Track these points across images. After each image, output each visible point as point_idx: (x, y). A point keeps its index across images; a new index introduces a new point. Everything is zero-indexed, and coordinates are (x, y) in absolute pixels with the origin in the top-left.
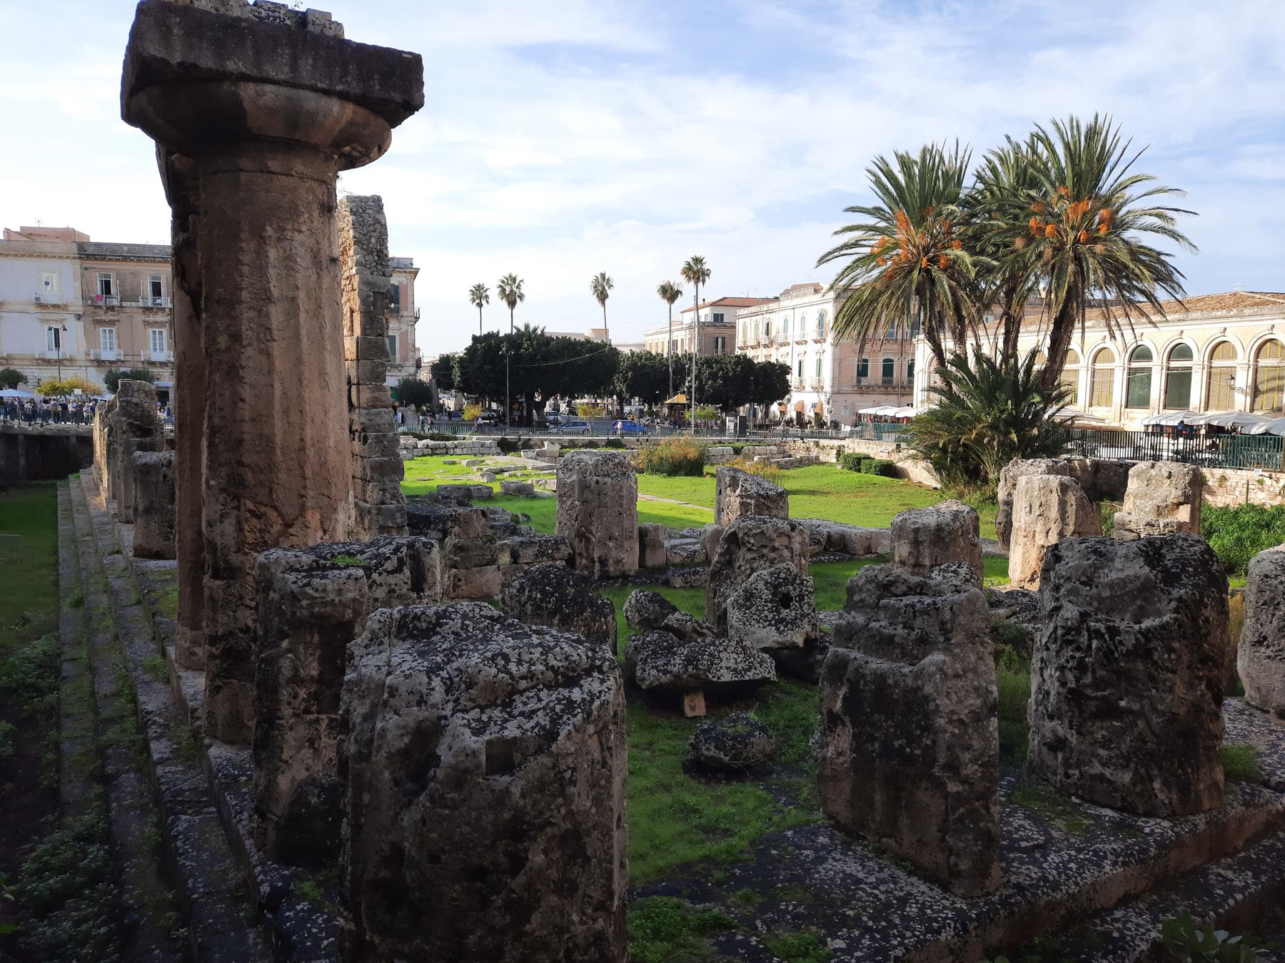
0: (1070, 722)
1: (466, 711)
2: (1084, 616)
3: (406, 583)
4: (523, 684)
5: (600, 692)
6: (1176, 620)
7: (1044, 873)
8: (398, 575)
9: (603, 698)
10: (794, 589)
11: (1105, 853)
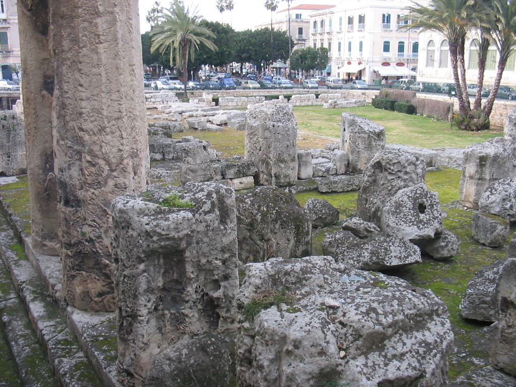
4: (390, 331)
10: (427, 201)
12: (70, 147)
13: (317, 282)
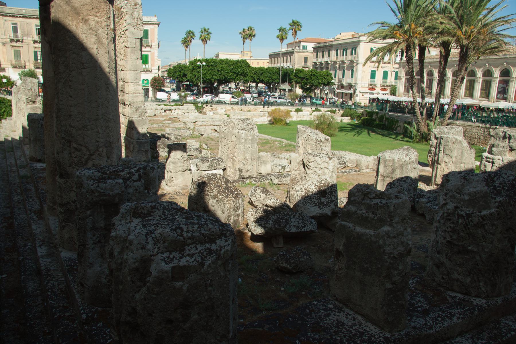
0: (446, 255)
1: (162, 253)
2: (456, 208)
3: (142, 186)
5: (225, 246)
6: (497, 211)
7: (426, 322)
8: (138, 182)
9: (226, 249)
11: (455, 313)
12: (63, 138)
13: (159, 214)
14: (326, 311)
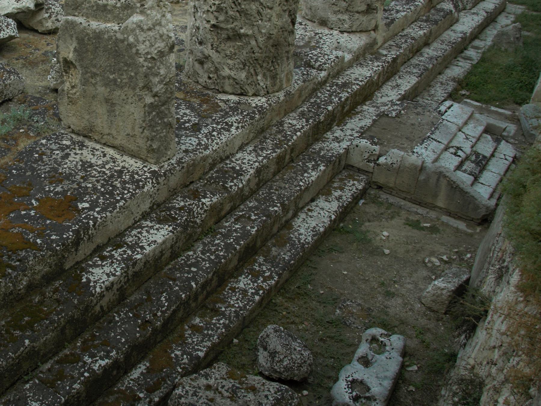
14: (63, 151)
